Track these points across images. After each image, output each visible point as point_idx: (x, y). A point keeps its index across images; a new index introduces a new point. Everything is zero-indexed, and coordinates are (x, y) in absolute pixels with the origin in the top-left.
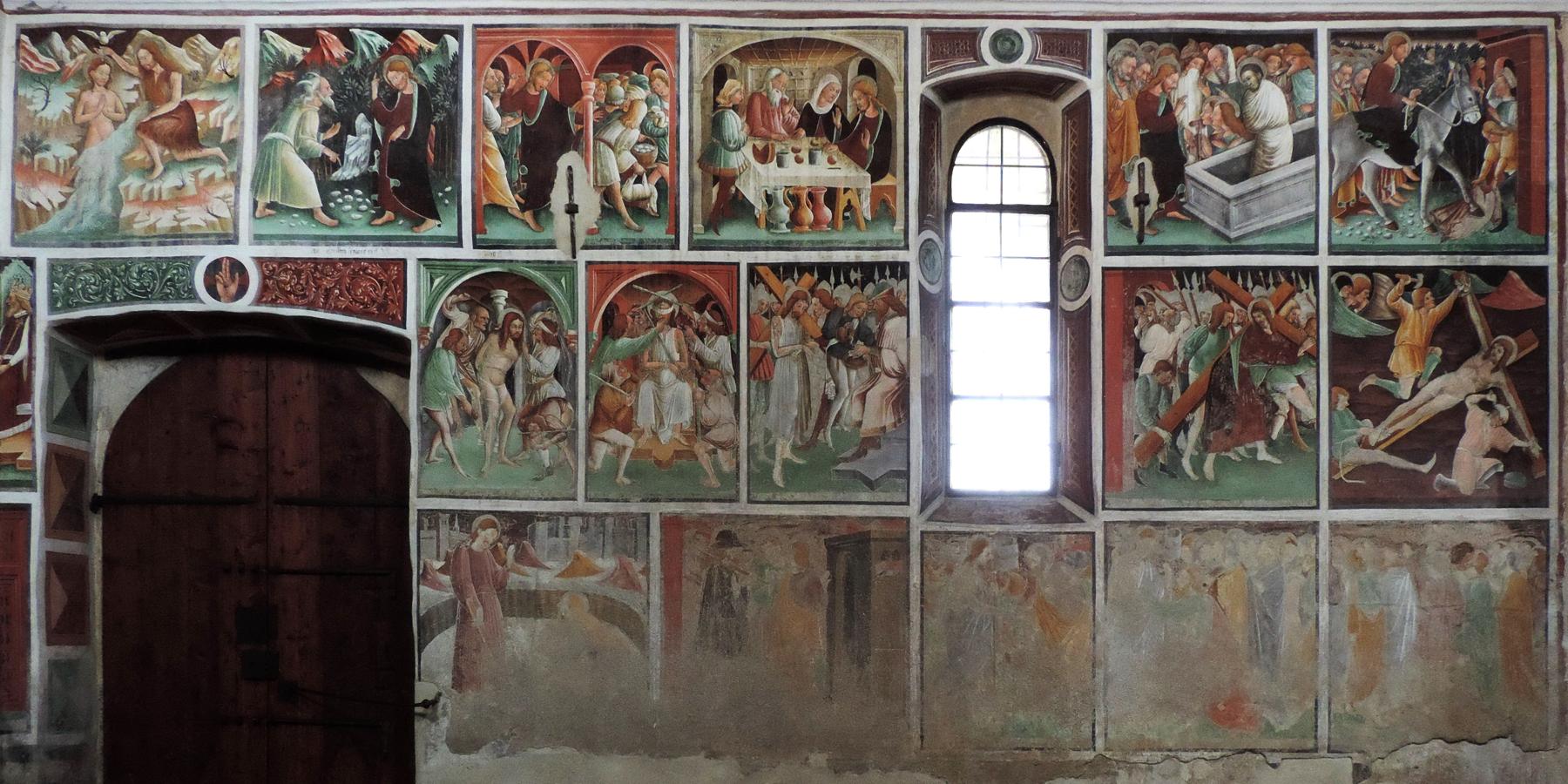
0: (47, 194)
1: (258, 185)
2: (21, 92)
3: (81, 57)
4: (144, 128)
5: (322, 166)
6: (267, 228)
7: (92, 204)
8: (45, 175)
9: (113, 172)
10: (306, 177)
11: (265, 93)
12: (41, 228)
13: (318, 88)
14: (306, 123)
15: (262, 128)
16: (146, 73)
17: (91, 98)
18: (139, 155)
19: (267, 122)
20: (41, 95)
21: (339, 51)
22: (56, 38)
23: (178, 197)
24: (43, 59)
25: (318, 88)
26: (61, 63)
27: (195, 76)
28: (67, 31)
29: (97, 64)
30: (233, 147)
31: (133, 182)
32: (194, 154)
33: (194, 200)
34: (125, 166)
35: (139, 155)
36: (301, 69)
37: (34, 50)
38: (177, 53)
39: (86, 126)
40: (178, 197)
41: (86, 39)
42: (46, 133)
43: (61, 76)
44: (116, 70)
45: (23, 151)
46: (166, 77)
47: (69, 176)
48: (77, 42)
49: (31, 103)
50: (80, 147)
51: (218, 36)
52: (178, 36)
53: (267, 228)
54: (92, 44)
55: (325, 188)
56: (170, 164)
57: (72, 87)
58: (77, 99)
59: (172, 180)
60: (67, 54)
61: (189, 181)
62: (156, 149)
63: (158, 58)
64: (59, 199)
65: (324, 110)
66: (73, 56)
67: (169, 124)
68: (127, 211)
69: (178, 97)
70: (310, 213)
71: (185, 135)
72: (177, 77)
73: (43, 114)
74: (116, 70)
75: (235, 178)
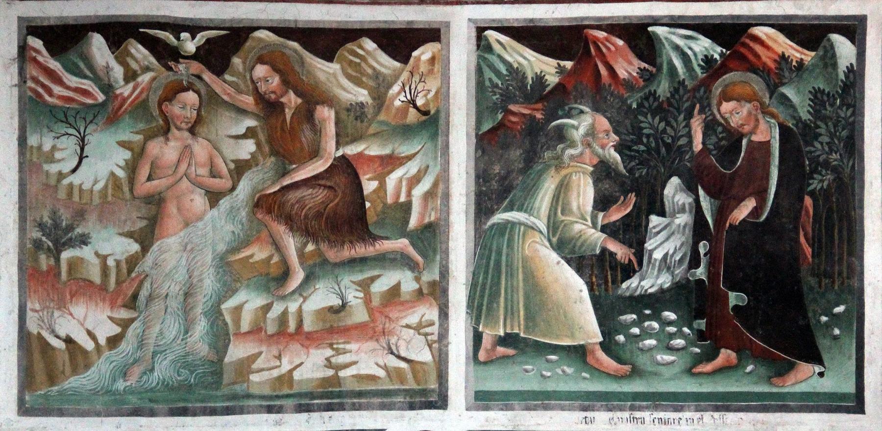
0: (86, 322)
1: (479, 307)
2: (33, 140)
3: (145, 78)
4: (266, 205)
5: (601, 272)
6: (498, 380)
7: (173, 338)
8: (83, 288)
9: (209, 284)
10: (572, 288)
11: (487, 142)
12: (73, 382)
13: (588, 129)
14: (571, 193)
15: (483, 206)
16: (270, 107)
17: (166, 151)
18: (259, 253)
19: (495, 192)
20: (68, 146)
21: (628, 67)
22: (98, 44)
23: (334, 327)
24: (73, 81)
25: (588, 129)
26: (107, 88)
27: (358, 111)
28: (118, 32)
29: (174, 91)
30: (431, 237)
31: (249, 301)
32: (361, 250)
33: (364, 331)
34: (231, 272)
35: (259, 253)
36: (557, 99)
37: (54, 65)
38: (325, 71)
40: (334, 327)
41: (154, 46)
42: (80, 215)
43: (109, 112)
44: (211, 101)
45: (38, 245)
46: (307, 114)
47: (126, 290)
48: (139, 51)
49: (50, 159)
50: (146, 238)
51: (400, 42)
52: (328, 41)
53: (498, 380)
54: (167, 54)
55: (607, 310)
57: (128, 133)
59: (322, 297)
60: (118, 72)
61: (354, 297)
62: (291, 243)
63: (290, 78)
64: (106, 330)
65: (602, 172)
66: (130, 76)
67: (315, 197)
68: (237, 352)
69: (331, 150)
70: (579, 353)
71: (344, 219)
72: (326, 114)
73: (75, 179)
75: (438, 292)
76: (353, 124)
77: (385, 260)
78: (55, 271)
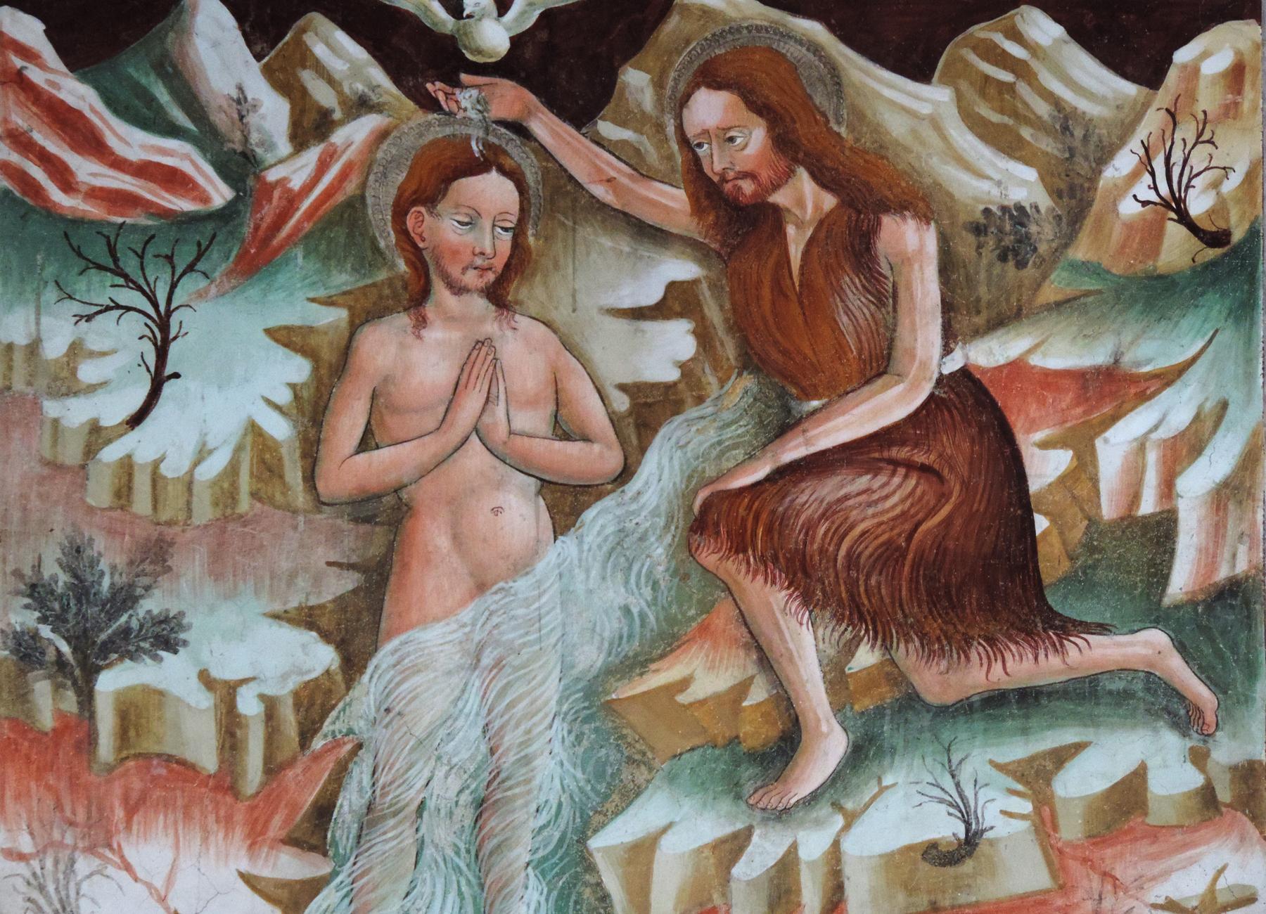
3: (354, 134)
4: (724, 522)
9: (551, 771)
16: (736, 222)
17: (417, 357)
18: (706, 674)
20: (121, 342)
24: (133, 142)
26: (240, 165)
27: (1007, 233)
32: (1022, 666)
34: (620, 734)
35: (706, 674)
37: (78, 93)
39: (384, 517)
42: (156, 555)
43: (240, 236)
44: (555, 201)
45: (27, 651)
49: (65, 383)
50: (355, 629)
56: (887, 724)
57: (302, 297)
58: (333, 367)
60: (273, 114)
61: (1003, 813)
62: (805, 644)
63: (799, 134)
66: (311, 126)
69: (927, 354)
72: (910, 243)
73: (142, 445)
74: (555, 201)
76: (995, 266)
77: (1089, 696)
78: (79, 732)
